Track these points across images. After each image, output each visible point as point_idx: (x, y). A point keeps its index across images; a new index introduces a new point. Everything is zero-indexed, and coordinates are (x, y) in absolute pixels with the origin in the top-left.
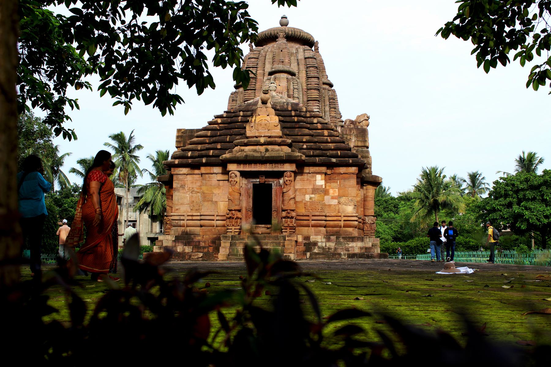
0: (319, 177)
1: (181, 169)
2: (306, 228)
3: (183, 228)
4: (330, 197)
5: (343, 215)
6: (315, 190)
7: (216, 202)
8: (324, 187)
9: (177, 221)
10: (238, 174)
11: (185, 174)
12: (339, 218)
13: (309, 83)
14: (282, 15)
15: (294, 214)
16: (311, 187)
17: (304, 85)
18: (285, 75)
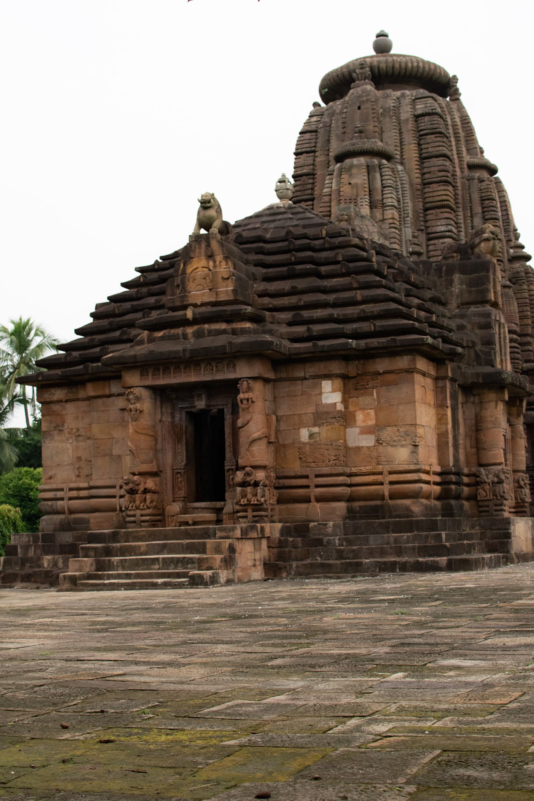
0: (327, 385)
2: (304, 506)
3: (62, 516)
4: (357, 430)
5: (387, 468)
6: (322, 416)
7: (119, 457)
8: (340, 407)
9: (50, 503)
10: (145, 393)
11: (60, 401)
12: (379, 478)
13: (425, 170)
14: (378, 31)
15: (260, 475)
16: (311, 409)
17: (416, 175)
18: (362, 160)
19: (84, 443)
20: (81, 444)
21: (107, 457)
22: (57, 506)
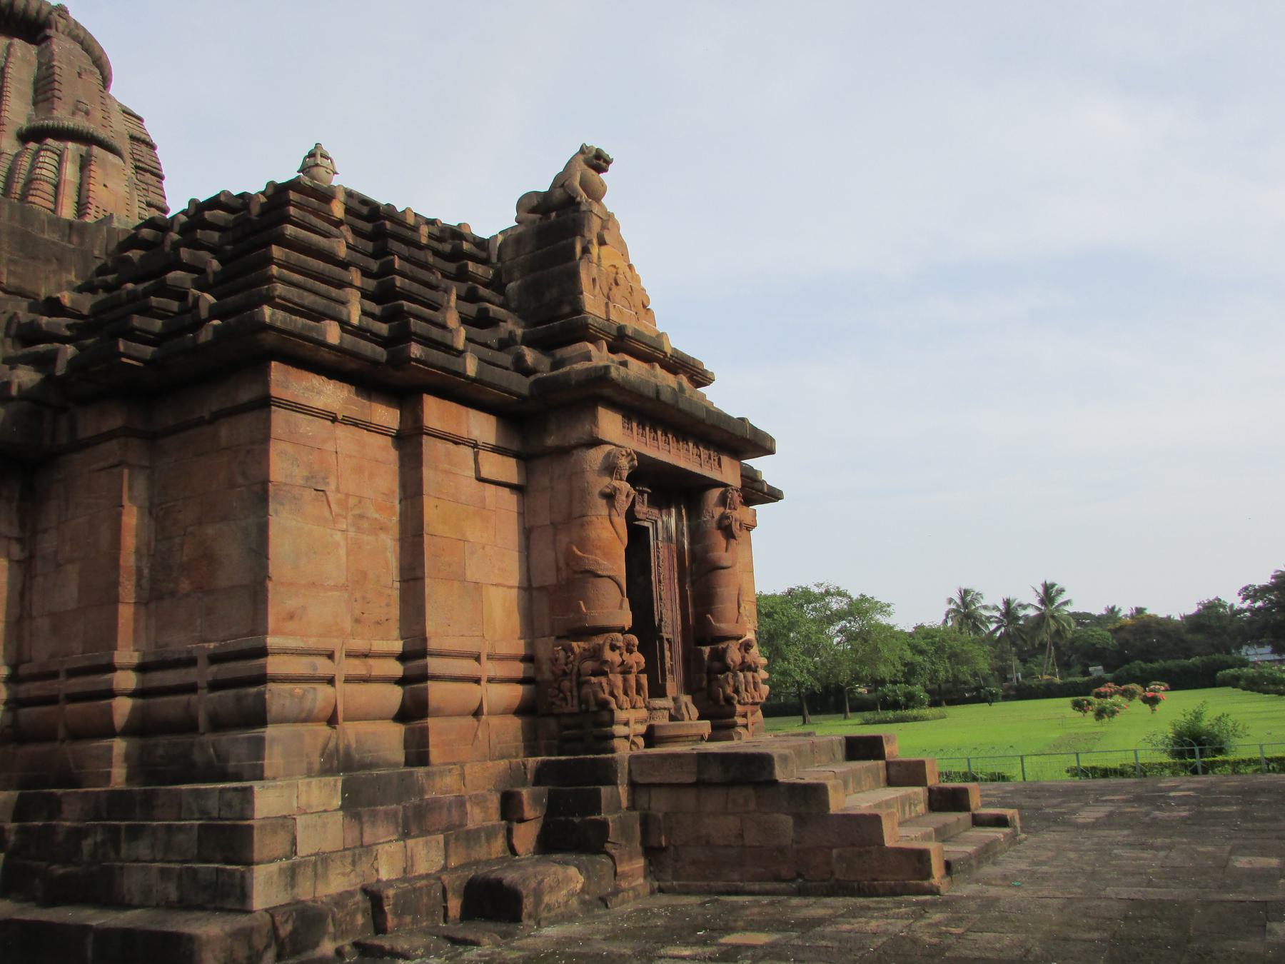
1: (317, 381)
9: (298, 689)
19: (371, 538)
20: (366, 538)
21: (456, 584)
22: (315, 700)
